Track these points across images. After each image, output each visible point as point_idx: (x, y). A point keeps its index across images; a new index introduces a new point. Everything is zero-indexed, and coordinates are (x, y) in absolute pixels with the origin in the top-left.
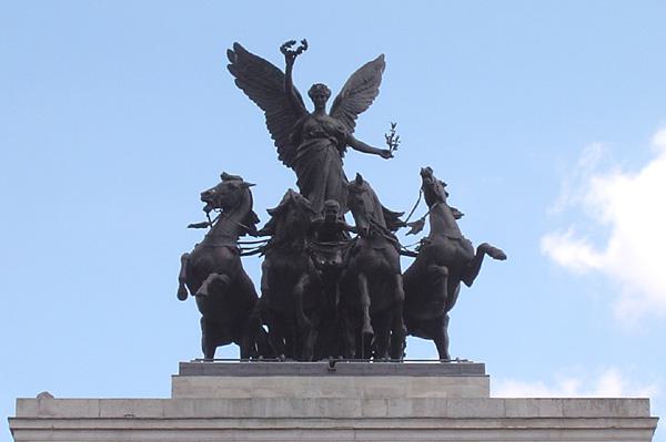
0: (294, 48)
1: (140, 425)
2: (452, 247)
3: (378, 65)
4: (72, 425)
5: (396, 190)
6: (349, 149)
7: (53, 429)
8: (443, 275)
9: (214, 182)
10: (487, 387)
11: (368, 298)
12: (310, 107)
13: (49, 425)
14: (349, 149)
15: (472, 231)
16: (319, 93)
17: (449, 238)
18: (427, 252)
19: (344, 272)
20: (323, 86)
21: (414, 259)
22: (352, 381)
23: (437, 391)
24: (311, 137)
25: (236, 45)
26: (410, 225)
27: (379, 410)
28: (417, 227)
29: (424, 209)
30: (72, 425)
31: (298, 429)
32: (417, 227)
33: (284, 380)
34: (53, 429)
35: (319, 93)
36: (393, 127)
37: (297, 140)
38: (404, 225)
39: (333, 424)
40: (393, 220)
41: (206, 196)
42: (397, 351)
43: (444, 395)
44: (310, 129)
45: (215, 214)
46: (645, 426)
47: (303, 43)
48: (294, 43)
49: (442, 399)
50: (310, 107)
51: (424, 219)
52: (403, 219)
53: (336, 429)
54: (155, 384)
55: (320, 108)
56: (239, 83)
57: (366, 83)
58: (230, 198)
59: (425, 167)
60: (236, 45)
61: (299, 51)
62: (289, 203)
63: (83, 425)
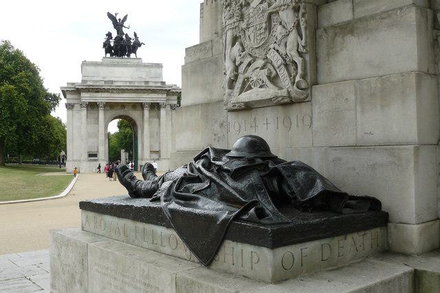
5: (131, 36)
15: (141, 40)
16: (120, 20)
23: (136, 61)
35: (120, 20)
40: (130, 39)
42: (128, 55)
54: (99, 59)
57: (125, 18)
58: (109, 35)
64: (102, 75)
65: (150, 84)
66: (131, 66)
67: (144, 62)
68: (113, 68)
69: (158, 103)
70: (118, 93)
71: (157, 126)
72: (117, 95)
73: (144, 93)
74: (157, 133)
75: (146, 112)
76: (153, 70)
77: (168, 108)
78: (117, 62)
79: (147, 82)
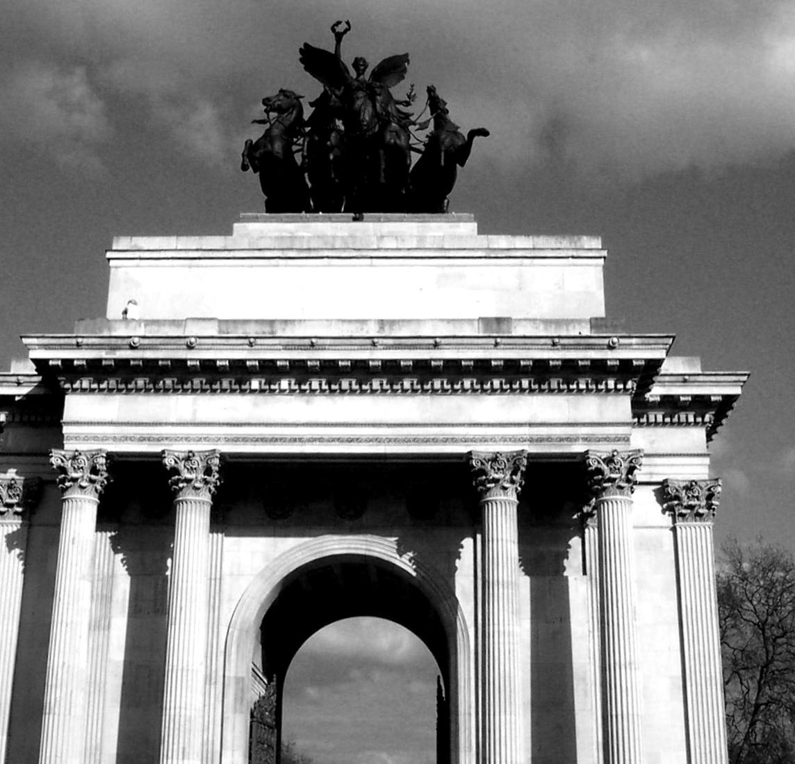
0: (340, 29)
3: (404, 58)
7: (141, 259)
9: (272, 92)
11: (383, 163)
12: (353, 73)
13: (137, 255)
18: (434, 140)
21: (420, 155)
22: (371, 225)
25: (306, 45)
26: (420, 124)
28: (423, 126)
31: (328, 257)
32: (423, 126)
33: (319, 224)
34: (141, 259)
35: (359, 64)
36: (412, 86)
38: (414, 124)
41: (266, 101)
43: (442, 234)
45: (273, 115)
46: (597, 255)
47: (348, 23)
48: (339, 23)
49: (440, 237)
50: (353, 73)
51: (429, 121)
52: (413, 118)
55: (359, 75)
56: (306, 69)
57: (394, 67)
59: (430, 85)
60: (306, 45)
62: (325, 96)
65: (519, 331)
77: (645, 498)
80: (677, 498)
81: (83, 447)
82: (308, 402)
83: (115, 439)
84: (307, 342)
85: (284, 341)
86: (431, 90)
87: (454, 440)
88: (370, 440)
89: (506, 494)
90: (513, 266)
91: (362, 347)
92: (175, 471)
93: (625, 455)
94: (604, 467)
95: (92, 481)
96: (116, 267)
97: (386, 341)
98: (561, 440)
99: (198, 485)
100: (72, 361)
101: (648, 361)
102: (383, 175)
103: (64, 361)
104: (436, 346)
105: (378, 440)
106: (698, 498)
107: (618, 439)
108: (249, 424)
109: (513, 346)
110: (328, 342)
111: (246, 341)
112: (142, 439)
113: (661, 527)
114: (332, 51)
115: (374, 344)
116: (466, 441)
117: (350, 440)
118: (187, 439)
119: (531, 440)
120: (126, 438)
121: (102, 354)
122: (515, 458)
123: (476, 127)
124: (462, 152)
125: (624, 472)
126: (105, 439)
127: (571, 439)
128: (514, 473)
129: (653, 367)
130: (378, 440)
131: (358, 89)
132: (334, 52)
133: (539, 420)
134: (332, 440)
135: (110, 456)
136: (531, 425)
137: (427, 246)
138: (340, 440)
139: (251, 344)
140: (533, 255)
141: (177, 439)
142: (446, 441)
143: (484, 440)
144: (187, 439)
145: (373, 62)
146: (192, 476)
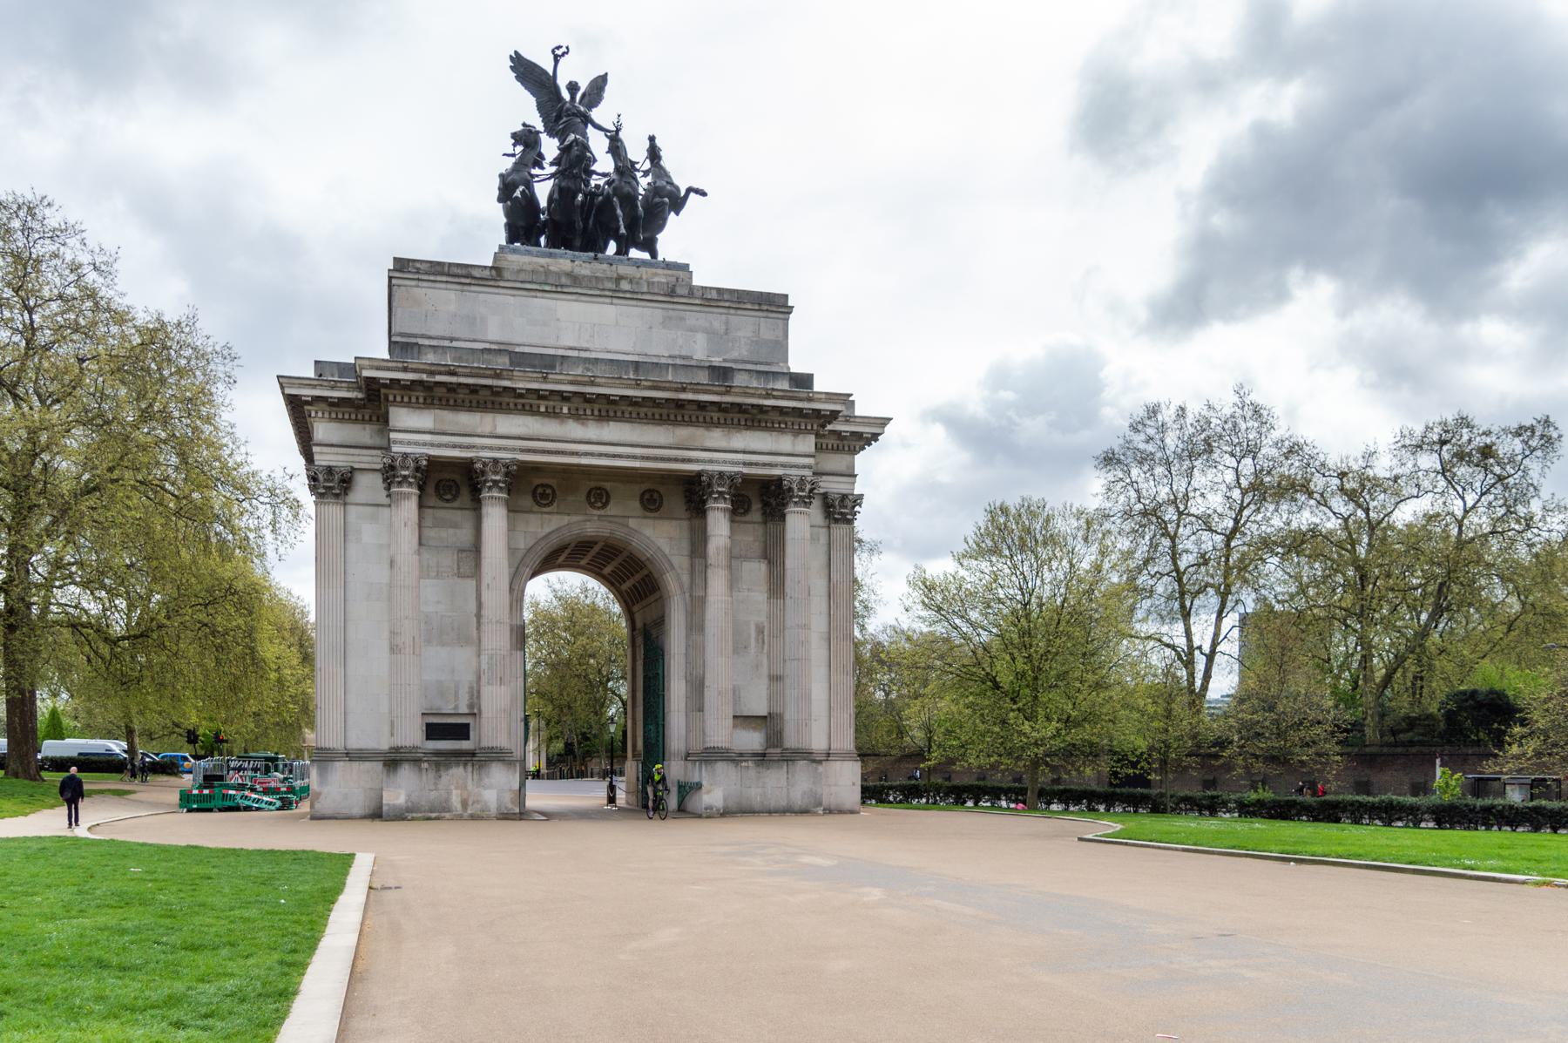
0: (559, 52)
1: (476, 282)
2: (668, 187)
4: (432, 278)
6: (589, 126)
7: (418, 279)
8: (664, 203)
10: (691, 278)
11: (619, 212)
13: (416, 276)
14: (589, 126)
16: (573, 87)
17: (667, 183)
18: (655, 190)
19: (601, 198)
20: (576, 83)
24: (569, 115)
25: (516, 52)
27: (625, 285)
28: (646, 173)
29: (647, 165)
30: (432, 278)
32: (646, 173)
34: (418, 279)
35: (573, 87)
37: (559, 117)
38: (638, 171)
39: (598, 293)
42: (627, 253)
43: (664, 280)
44: (568, 110)
47: (567, 48)
50: (566, 95)
52: (637, 166)
53: (600, 296)
56: (517, 78)
57: (599, 84)
60: (516, 52)
61: (563, 54)
63: (439, 278)
64: (491, 337)
66: (635, 296)
67: (697, 281)
68: (541, 303)
69: (780, 479)
70: (576, 416)
71: (760, 596)
72: (574, 429)
73: (710, 424)
74: (760, 631)
75: (719, 524)
76: (746, 326)
78: (569, 275)
79: (722, 374)
80: (833, 506)
81: (409, 450)
82: (583, 424)
83: (432, 445)
84: (586, 379)
85: (570, 378)
86: (652, 139)
87: (689, 461)
88: (628, 457)
89: (725, 503)
90: (721, 314)
91: (628, 387)
92: (483, 473)
93: (809, 479)
94: (794, 486)
95: (415, 477)
96: (399, 286)
97: (645, 383)
98: (765, 465)
99: (501, 485)
100: (399, 380)
101: (832, 411)
102: (622, 227)
103: (391, 380)
104: (684, 390)
105: (634, 457)
106: (846, 507)
107: (804, 467)
108: (539, 440)
109: (737, 394)
110: (603, 380)
111: (540, 375)
112: (455, 446)
113: (819, 527)
114: (551, 74)
115: (638, 385)
116: (697, 461)
117: (614, 456)
118: (491, 448)
119: (745, 464)
120: (440, 446)
121: (424, 377)
122: (732, 477)
123: (695, 186)
124: (678, 203)
125: (807, 490)
126: (425, 444)
127: (771, 465)
128: (730, 488)
129: (834, 415)
130: (634, 457)
131: (574, 114)
132: (551, 74)
133: (751, 449)
134: (600, 455)
135: (429, 456)
136: (744, 452)
137: (656, 291)
138: (607, 455)
139: (545, 378)
140: (738, 306)
141: (484, 448)
142: (684, 461)
143: (711, 461)
144: (491, 448)
145: (583, 86)
146: (498, 478)
